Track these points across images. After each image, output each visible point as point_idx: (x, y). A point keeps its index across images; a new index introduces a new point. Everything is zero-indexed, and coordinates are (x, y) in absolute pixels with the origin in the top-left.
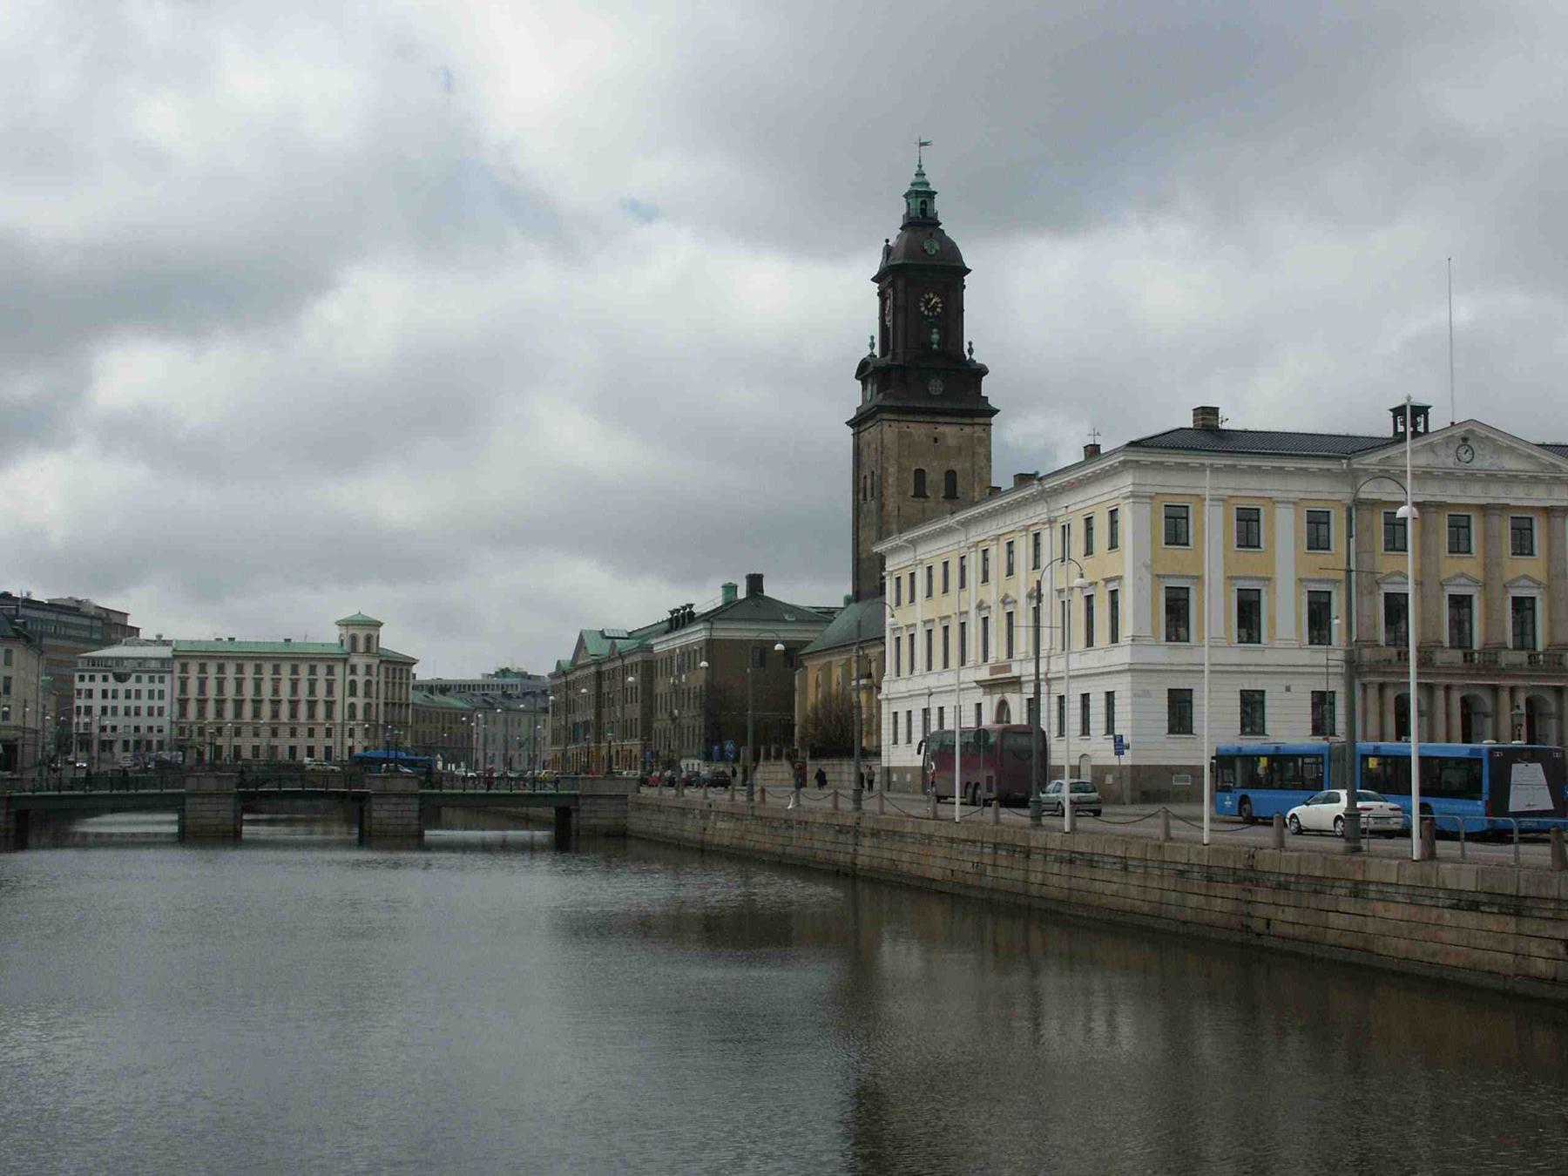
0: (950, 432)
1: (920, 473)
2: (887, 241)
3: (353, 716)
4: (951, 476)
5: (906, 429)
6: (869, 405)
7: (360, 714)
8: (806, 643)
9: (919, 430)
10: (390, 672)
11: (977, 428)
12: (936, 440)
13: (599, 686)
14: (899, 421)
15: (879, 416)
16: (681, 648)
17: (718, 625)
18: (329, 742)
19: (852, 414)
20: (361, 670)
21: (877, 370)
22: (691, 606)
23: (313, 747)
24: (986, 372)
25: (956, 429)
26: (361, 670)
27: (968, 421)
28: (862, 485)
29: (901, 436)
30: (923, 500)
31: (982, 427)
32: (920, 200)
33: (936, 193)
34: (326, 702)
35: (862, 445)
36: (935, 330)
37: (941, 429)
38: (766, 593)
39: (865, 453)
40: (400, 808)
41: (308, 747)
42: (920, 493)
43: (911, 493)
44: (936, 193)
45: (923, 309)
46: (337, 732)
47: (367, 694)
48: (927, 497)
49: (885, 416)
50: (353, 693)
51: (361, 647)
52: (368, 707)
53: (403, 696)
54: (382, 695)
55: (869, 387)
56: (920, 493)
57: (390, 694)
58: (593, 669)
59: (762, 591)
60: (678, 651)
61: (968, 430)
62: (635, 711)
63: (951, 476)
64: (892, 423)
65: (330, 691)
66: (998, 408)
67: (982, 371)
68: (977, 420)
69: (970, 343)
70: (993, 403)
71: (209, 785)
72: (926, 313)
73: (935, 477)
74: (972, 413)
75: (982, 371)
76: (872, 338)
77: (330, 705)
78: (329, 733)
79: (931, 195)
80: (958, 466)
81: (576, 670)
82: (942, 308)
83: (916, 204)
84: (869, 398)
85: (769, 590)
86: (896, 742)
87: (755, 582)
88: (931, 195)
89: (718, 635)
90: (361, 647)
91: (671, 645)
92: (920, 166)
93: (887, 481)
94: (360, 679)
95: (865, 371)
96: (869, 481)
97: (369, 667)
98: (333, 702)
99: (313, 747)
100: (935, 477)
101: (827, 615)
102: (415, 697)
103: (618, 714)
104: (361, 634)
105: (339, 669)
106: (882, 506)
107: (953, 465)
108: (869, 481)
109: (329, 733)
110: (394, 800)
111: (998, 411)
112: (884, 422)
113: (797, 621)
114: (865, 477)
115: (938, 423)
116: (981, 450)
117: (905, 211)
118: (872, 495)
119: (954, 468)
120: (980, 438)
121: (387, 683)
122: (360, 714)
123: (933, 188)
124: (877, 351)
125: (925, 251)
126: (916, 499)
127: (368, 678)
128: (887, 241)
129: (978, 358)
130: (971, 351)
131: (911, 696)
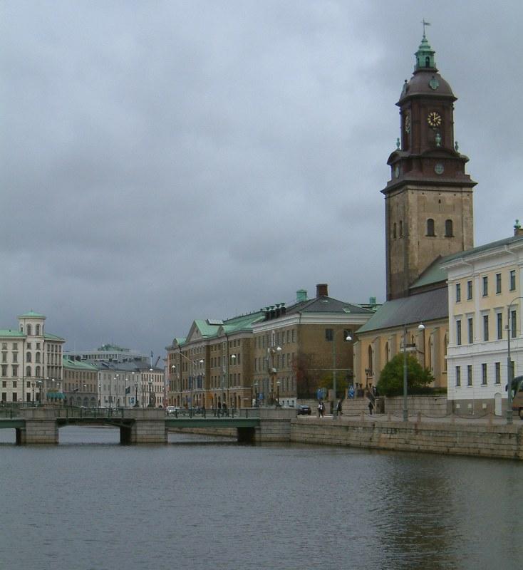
0: (448, 196)
1: (431, 222)
2: (406, 81)
3: (29, 374)
4: (449, 222)
6: (398, 181)
7: (33, 373)
8: (360, 326)
9: (430, 195)
10: (51, 347)
11: (465, 194)
12: (440, 202)
13: (208, 355)
14: (418, 190)
15: (404, 188)
16: (276, 330)
17: (304, 315)
18: (15, 390)
19: (384, 186)
20: (34, 346)
21: (403, 159)
22: (283, 304)
23: (6, 393)
24: (468, 160)
25: (451, 194)
26: (34, 346)
27: (459, 189)
28: (392, 229)
29: (419, 199)
30: (432, 238)
32: (425, 56)
33: (434, 52)
34: (13, 366)
35: (392, 204)
36: (438, 135)
37: (443, 194)
38: (329, 296)
39: (395, 209)
40: (154, 428)
41: (14, 393)
42: (431, 234)
43: (426, 233)
44: (434, 52)
45: (430, 122)
46: (20, 384)
47: (38, 361)
48: (435, 236)
49: (409, 187)
50: (29, 360)
51: (34, 332)
52: (38, 368)
53: (58, 363)
54: (46, 362)
55: (397, 169)
56: (431, 234)
57: (50, 362)
58: (204, 344)
59: (327, 295)
60: (273, 332)
61: (459, 195)
62: (239, 369)
63: (449, 222)
64: (414, 191)
65: (15, 359)
66: (477, 182)
67: (465, 160)
68: (464, 189)
69: (456, 143)
70: (473, 179)
71: (40, 415)
72: (432, 124)
73: (440, 225)
74: (461, 185)
75: (465, 160)
76: (398, 139)
77: (15, 367)
78: (15, 385)
79: (432, 53)
81: (189, 344)
82: (441, 121)
83: (423, 59)
84: (397, 176)
85: (331, 294)
86: (458, 384)
87: (322, 289)
88: (432, 53)
89: (304, 322)
90: (34, 332)
91: (268, 328)
92: (424, 37)
93: (411, 227)
94: (33, 351)
95: (393, 160)
96: (398, 227)
97: (38, 345)
98: (17, 366)
99: (6, 393)
100: (440, 225)
101: (369, 309)
102: (65, 362)
103: (224, 371)
104: (34, 324)
105: (20, 345)
106: (407, 242)
107: (450, 217)
108: (398, 227)
109: (15, 385)
110: (149, 424)
111: (476, 184)
113: (352, 313)
114: (395, 224)
116: (466, 207)
117: (415, 63)
118: (401, 235)
119: (450, 219)
120: (465, 200)
121: (48, 354)
122: (33, 373)
123: (432, 49)
124: (400, 147)
125: (430, 87)
126: (429, 237)
127: (38, 351)
128: (406, 81)
129: (462, 151)
130: (457, 147)
131: (472, 357)
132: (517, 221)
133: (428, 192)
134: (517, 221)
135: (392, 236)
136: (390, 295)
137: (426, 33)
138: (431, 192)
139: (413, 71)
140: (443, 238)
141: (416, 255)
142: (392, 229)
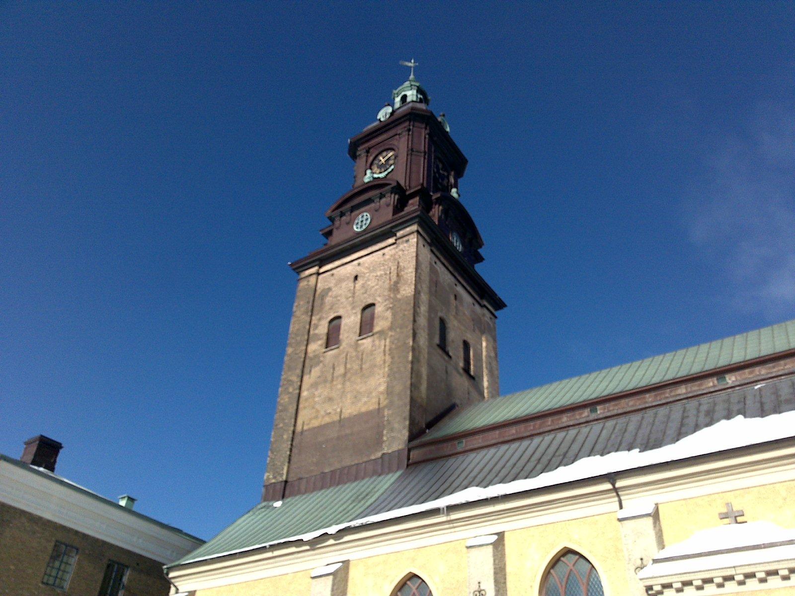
5: (434, 264)
11: (488, 315)
30: (446, 358)
31: (492, 317)
37: (459, 289)
43: (437, 340)
48: (450, 357)
61: (477, 307)
63: (466, 345)
64: (426, 244)
93: (419, 307)
96: (351, 321)
107: (470, 338)
115: (460, 282)
126: (440, 352)
133: (443, 269)
135: (315, 347)
136: (286, 482)
138: (446, 272)
140: (461, 371)
142: (322, 329)
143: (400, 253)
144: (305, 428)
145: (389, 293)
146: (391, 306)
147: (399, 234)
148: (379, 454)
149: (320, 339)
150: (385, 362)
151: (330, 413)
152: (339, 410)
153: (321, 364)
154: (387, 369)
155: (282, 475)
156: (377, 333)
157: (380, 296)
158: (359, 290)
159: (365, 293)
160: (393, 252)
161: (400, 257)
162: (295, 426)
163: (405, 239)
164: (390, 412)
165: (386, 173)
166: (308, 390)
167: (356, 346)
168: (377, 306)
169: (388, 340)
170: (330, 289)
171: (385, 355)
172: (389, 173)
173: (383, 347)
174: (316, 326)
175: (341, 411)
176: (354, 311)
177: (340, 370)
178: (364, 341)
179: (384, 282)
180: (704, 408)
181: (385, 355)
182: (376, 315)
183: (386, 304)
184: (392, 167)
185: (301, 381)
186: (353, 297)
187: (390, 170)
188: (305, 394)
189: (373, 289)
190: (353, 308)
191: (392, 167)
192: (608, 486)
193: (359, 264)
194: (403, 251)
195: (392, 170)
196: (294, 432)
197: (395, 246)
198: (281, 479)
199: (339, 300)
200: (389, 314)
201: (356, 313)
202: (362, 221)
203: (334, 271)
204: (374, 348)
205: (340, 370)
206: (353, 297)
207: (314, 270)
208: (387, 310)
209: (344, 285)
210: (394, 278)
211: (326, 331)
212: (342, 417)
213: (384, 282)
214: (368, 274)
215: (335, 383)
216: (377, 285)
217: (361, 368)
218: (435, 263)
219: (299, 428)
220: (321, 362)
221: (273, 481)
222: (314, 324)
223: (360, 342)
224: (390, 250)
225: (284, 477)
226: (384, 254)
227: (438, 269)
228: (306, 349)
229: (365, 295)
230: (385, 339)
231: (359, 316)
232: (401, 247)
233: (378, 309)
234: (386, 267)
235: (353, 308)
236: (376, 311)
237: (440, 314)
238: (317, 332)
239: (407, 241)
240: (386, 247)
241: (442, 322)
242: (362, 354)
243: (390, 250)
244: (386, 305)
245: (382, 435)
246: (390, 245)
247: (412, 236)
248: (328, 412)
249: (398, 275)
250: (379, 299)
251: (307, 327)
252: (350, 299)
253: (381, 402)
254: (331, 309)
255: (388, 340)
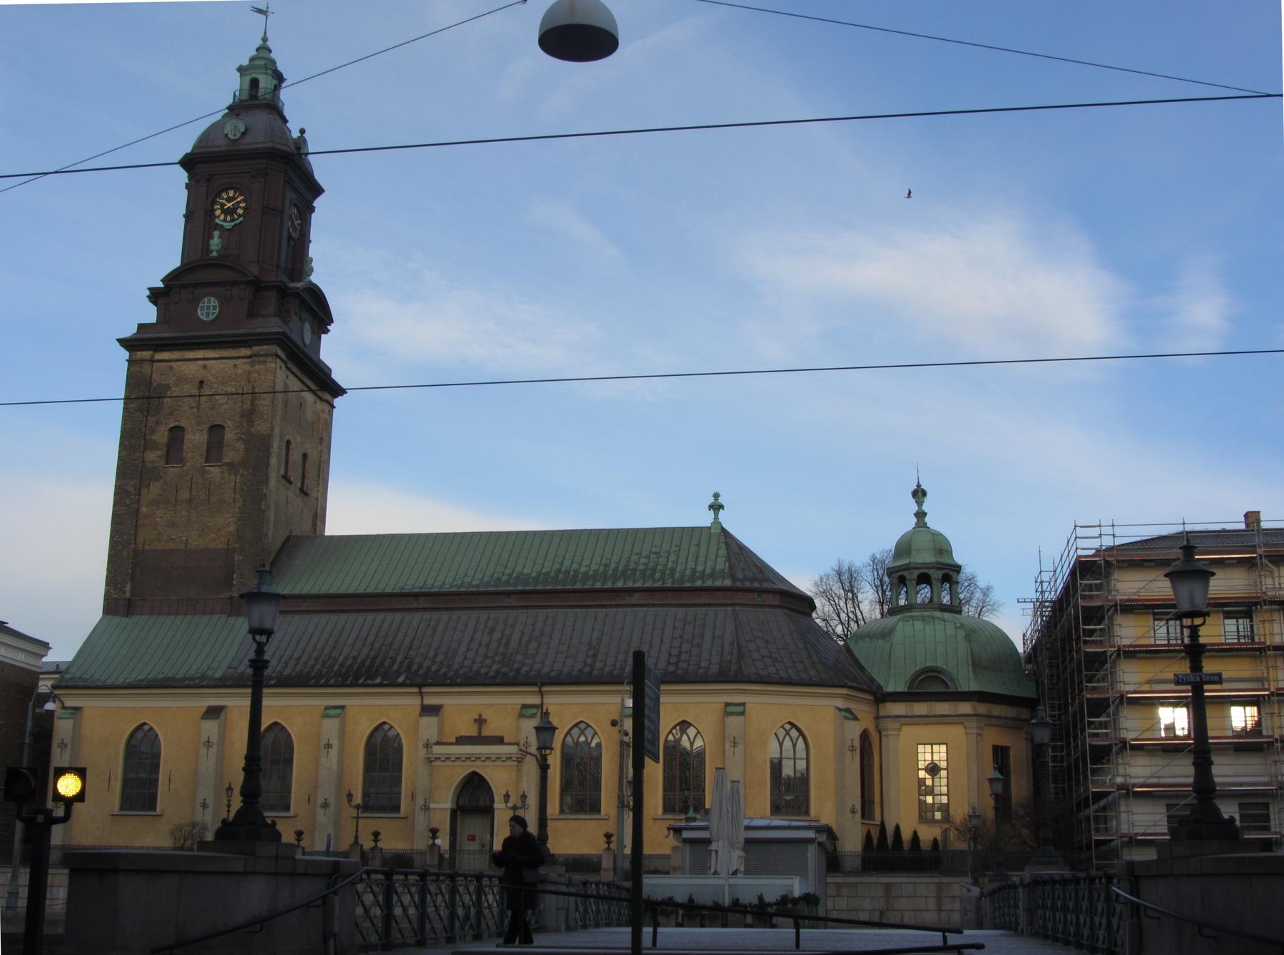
11: (326, 407)
14: (287, 367)
19: (130, 331)
30: (287, 485)
43: (282, 472)
48: (291, 483)
68: (327, 396)
73: (296, 457)
80: (313, 454)
92: (265, 40)
93: (272, 446)
96: (196, 438)
112: (278, 360)
126: (284, 482)
132: (716, 496)
134: (716, 496)
135: (152, 456)
137: (268, 35)
139: (229, 101)
140: (298, 491)
141: (272, 515)
142: (162, 436)
143: (256, 375)
144: (146, 548)
145: (241, 419)
146: (243, 436)
147: (256, 349)
148: (229, 594)
149: (157, 449)
150: (234, 501)
151: (174, 539)
152: (184, 538)
153: (161, 481)
154: (237, 510)
155: (125, 593)
156: (225, 464)
157: (230, 419)
158: (205, 402)
159: (213, 408)
160: (247, 367)
161: (255, 381)
162: (135, 543)
163: (261, 358)
164: (241, 558)
165: (232, 224)
166: (147, 506)
167: (203, 472)
168: (227, 430)
169: (239, 477)
170: (168, 387)
171: (235, 493)
172: (235, 225)
173: (233, 483)
174: (153, 432)
175: (187, 540)
176: (199, 428)
177: (184, 495)
178: (210, 468)
179: (235, 404)
180: (491, 623)
181: (235, 493)
182: (225, 442)
183: (237, 431)
184: (241, 219)
185: (139, 494)
186: (198, 409)
187: (237, 222)
188: (144, 509)
189: (223, 407)
190: (199, 423)
191: (241, 219)
192: (416, 690)
193: (205, 367)
194: (260, 375)
195: (241, 222)
196: (134, 550)
197: (249, 360)
198: (122, 597)
199: (180, 406)
200: (240, 446)
201: (202, 430)
202: (208, 308)
203: (174, 365)
204: (223, 481)
205: (184, 495)
206: (198, 409)
207: (146, 354)
208: (238, 440)
209: (186, 387)
210: (248, 406)
211: (166, 440)
212: (188, 547)
213: (235, 404)
214: (216, 385)
215: (178, 507)
216: (227, 403)
217: (209, 500)
218: (287, 377)
219: (140, 546)
220: (162, 477)
221: (115, 596)
222: (151, 427)
223: (207, 468)
224: (245, 363)
225: (128, 595)
226: (235, 366)
227: (289, 382)
228: (143, 458)
229: (213, 412)
230: (236, 475)
231: (206, 437)
232: (257, 367)
233: (229, 435)
234: (238, 384)
235: (199, 423)
236: (226, 437)
237: (287, 438)
238: (154, 438)
239: (264, 362)
240: (239, 358)
241: (288, 442)
242: (210, 484)
243: (245, 363)
244: (235, 434)
245: (232, 579)
246: (243, 358)
247: (270, 359)
248: (173, 537)
249: (252, 404)
250: (228, 421)
251: (144, 430)
252: (195, 410)
253: (230, 543)
254: (171, 414)
255: (239, 477)
